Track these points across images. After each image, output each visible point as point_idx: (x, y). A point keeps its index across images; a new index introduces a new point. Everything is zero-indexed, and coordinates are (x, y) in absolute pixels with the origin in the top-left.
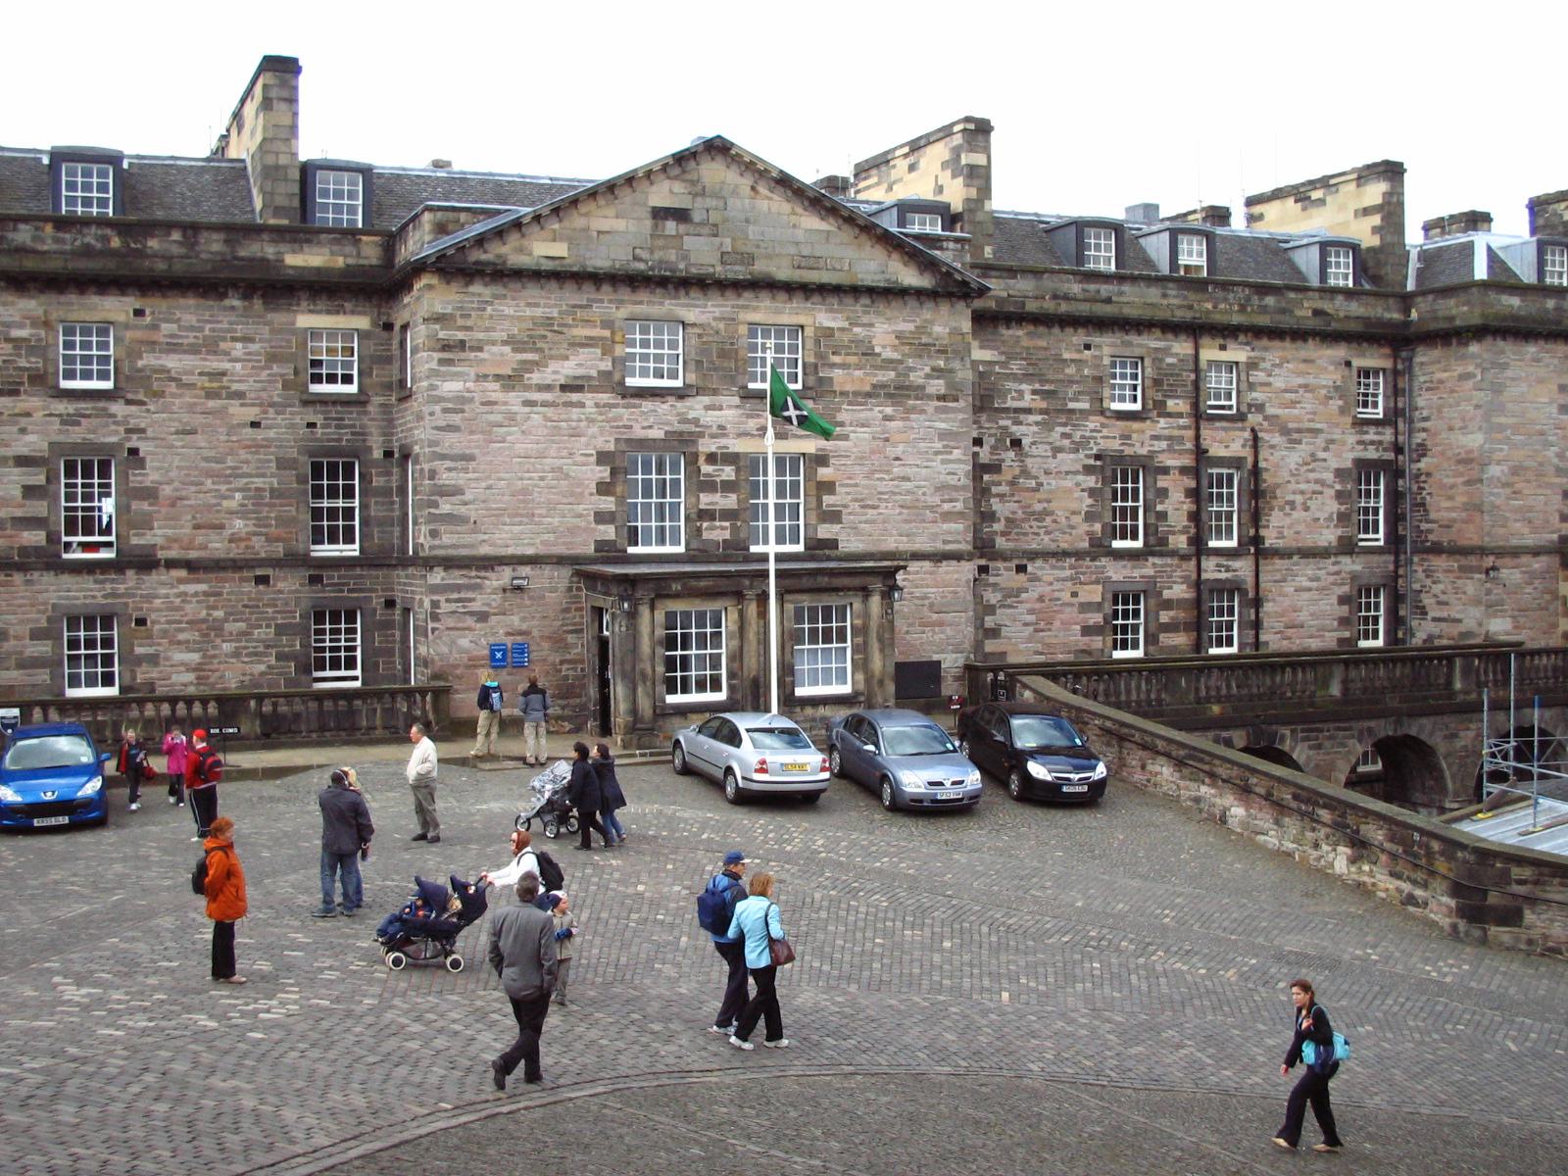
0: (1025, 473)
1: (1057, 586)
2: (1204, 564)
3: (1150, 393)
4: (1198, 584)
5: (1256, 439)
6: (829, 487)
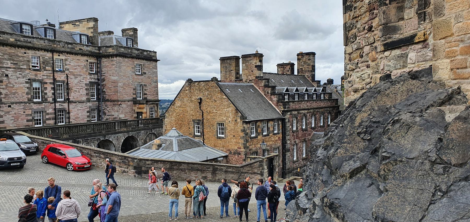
0: (10, 83)
1: (19, 110)
2: (56, 105)
3: (42, 65)
4: (55, 109)
5: (67, 76)
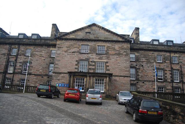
4: (173, 87)
5: (181, 67)
6: (108, 66)
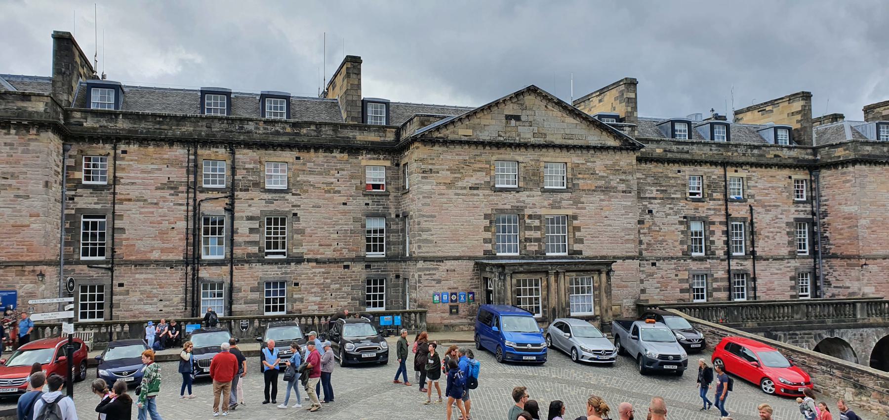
0: (654, 224)
1: (669, 272)
2: (731, 263)
3: (706, 191)
4: (729, 271)
5: (751, 210)
6: (578, 229)
